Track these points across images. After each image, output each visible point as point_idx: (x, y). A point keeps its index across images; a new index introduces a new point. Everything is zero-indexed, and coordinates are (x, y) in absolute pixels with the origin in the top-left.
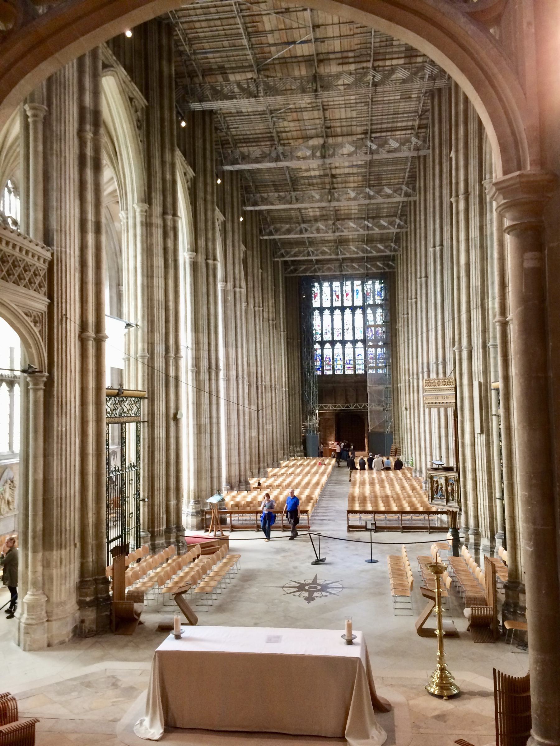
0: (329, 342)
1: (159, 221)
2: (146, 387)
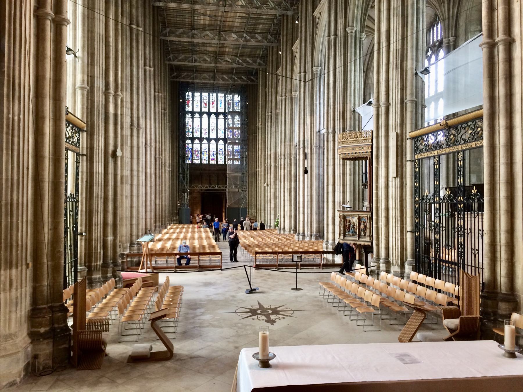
0: (198, 138)
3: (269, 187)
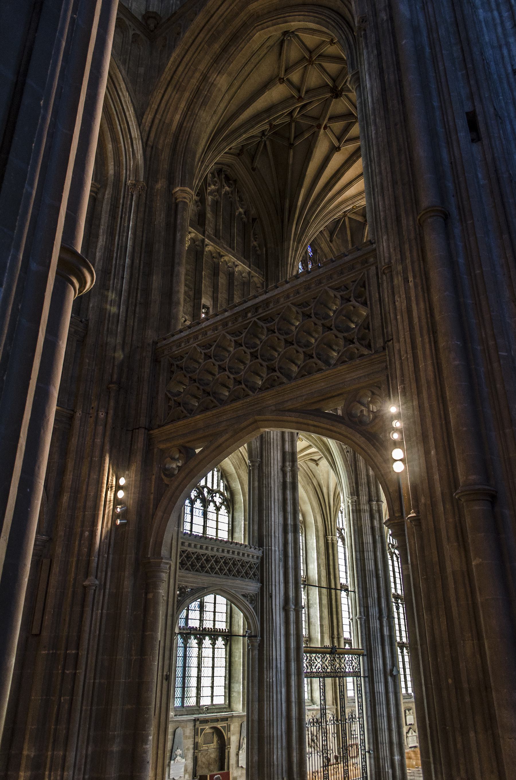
1: (366, 507)
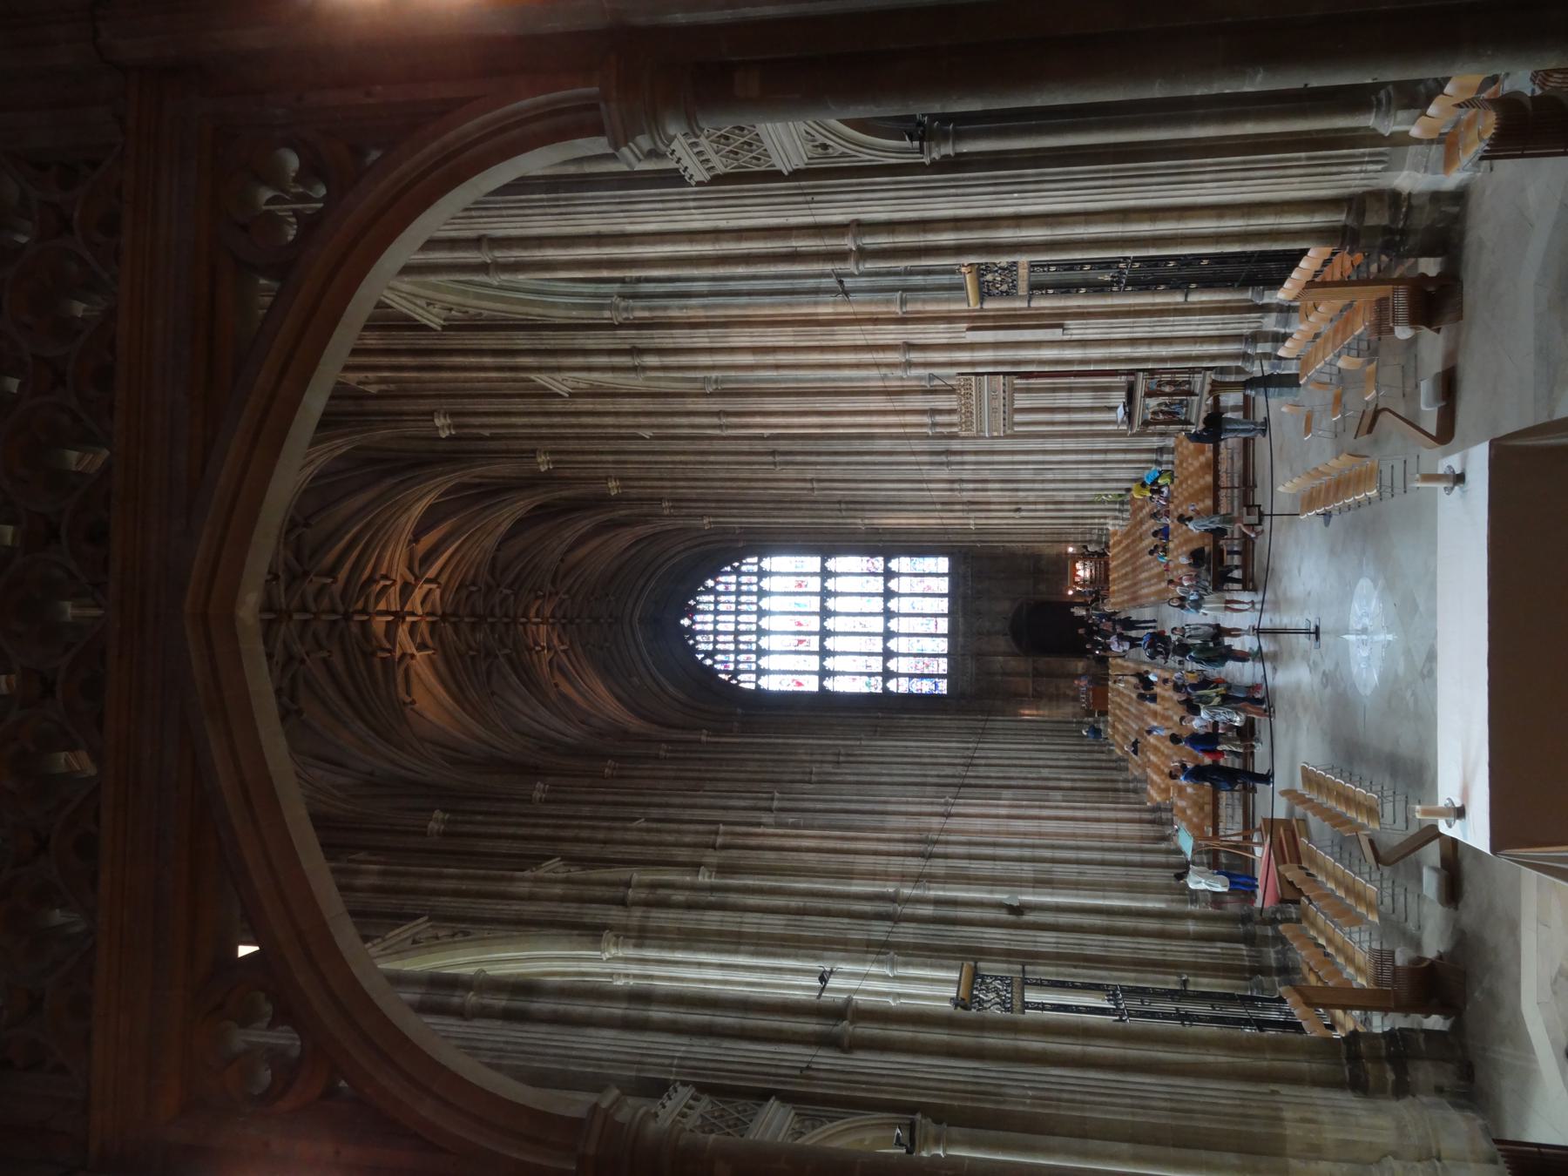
0: (885, 661)
1: (637, 912)
2: (953, 962)
3: (1023, 507)
